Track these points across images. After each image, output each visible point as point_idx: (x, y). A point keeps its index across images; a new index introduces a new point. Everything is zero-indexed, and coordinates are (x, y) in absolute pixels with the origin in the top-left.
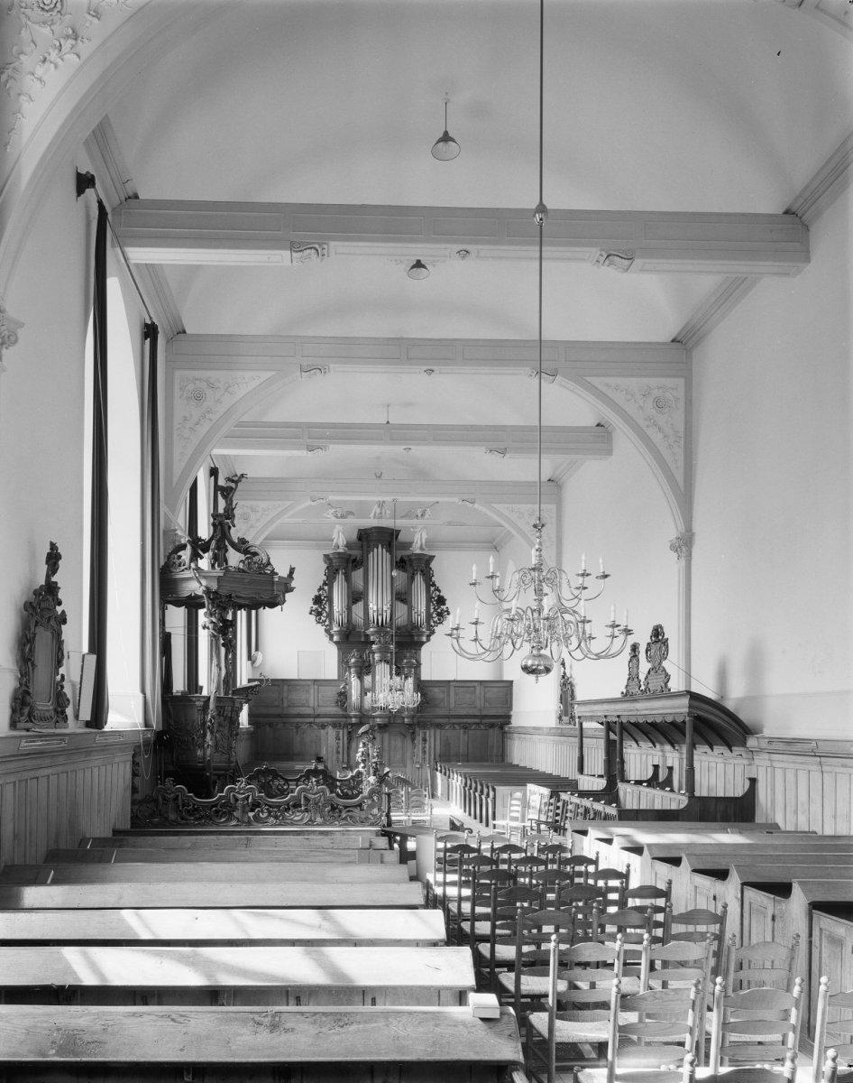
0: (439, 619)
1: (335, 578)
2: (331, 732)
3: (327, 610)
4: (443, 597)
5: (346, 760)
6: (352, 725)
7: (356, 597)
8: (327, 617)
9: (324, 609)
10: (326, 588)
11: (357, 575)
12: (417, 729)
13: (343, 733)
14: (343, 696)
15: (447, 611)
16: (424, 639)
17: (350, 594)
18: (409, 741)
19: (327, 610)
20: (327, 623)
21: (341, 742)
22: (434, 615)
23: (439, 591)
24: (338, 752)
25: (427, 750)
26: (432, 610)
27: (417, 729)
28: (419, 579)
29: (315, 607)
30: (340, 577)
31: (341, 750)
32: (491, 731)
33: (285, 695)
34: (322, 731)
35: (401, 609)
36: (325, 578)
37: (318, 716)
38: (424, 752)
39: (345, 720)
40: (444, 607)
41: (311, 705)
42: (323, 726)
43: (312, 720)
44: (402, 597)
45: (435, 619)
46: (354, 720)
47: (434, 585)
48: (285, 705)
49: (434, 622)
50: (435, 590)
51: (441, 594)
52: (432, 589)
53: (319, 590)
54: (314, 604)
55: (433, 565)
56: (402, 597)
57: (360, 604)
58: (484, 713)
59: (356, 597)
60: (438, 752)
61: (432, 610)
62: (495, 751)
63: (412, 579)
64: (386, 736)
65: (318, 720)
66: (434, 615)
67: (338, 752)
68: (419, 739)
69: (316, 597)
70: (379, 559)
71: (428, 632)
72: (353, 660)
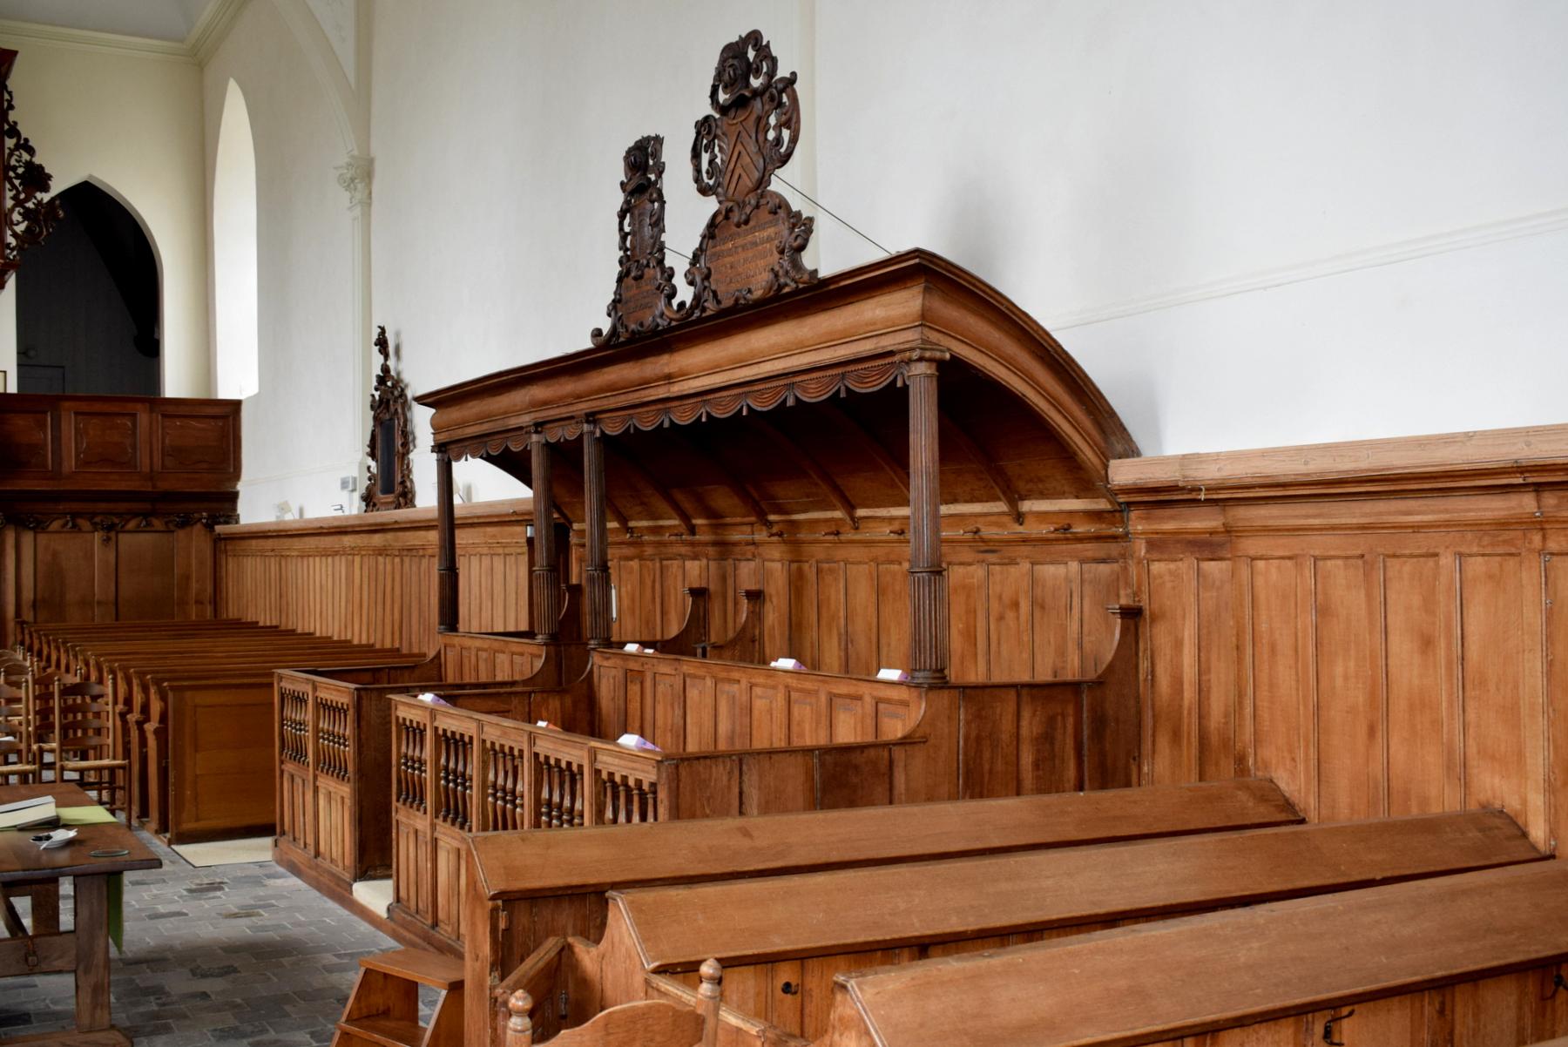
4: (41, 168)
22: (16, 217)
23: (31, 151)
26: (9, 203)
32: (181, 534)
47: (14, 132)
50: (18, 147)
51: (37, 160)
58: (164, 486)
60: (28, 594)
61: (9, 203)
62: (194, 586)
66: (16, 217)
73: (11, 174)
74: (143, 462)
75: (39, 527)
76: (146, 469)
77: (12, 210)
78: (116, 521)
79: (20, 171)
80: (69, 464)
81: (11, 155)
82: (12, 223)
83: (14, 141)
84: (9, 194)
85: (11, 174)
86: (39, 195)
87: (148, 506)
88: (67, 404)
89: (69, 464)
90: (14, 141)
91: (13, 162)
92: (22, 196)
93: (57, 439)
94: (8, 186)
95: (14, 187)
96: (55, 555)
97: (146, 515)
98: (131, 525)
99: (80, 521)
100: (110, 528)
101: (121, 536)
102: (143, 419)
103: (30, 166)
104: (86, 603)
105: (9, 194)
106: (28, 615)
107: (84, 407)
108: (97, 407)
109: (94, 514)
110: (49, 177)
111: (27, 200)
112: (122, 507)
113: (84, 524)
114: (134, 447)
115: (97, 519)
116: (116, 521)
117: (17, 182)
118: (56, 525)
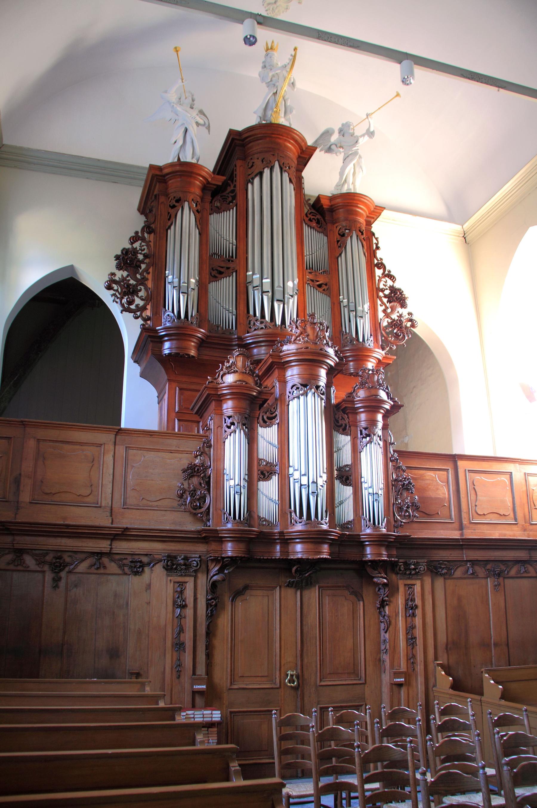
1: (171, 218)
5: (201, 670)
7: (218, 265)
8: (147, 300)
9: (142, 282)
11: (223, 224)
13: (197, 589)
14: (201, 477)
15: (411, 320)
19: (150, 284)
20: (148, 313)
21: (189, 612)
24: (179, 646)
25: (418, 633)
26: (381, 315)
29: (120, 274)
30: (186, 218)
31: (188, 637)
33: (27, 466)
37: (124, 534)
38: (411, 641)
39: (201, 548)
40: (404, 312)
41: (106, 502)
42: (137, 566)
43: (103, 545)
46: (230, 549)
47: (381, 265)
48: (25, 497)
50: (385, 275)
51: (397, 285)
52: (379, 272)
53: (134, 239)
54: (119, 267)
55: (375, 228)
60: (442, 638)
63: (337, 247)
64: (313, 595)
65: (122, 547)
67: (179, 646)
69: (125, 252)
72: (230, 379)
73: (381, 294)
78: (503, 568)
79: (387, 292)
81: (380, 281)
83: (381, 271)
85: (381, 294)
90: (381, 271)
91: (381, 286)
94: (379, 302)
98: (513, 572)
101: (506, 580)
103: (392, 288)
104: (485, 645)
105: (380, 309)
115: (488, 567)
116: (503, 568)
118: (458, 573)
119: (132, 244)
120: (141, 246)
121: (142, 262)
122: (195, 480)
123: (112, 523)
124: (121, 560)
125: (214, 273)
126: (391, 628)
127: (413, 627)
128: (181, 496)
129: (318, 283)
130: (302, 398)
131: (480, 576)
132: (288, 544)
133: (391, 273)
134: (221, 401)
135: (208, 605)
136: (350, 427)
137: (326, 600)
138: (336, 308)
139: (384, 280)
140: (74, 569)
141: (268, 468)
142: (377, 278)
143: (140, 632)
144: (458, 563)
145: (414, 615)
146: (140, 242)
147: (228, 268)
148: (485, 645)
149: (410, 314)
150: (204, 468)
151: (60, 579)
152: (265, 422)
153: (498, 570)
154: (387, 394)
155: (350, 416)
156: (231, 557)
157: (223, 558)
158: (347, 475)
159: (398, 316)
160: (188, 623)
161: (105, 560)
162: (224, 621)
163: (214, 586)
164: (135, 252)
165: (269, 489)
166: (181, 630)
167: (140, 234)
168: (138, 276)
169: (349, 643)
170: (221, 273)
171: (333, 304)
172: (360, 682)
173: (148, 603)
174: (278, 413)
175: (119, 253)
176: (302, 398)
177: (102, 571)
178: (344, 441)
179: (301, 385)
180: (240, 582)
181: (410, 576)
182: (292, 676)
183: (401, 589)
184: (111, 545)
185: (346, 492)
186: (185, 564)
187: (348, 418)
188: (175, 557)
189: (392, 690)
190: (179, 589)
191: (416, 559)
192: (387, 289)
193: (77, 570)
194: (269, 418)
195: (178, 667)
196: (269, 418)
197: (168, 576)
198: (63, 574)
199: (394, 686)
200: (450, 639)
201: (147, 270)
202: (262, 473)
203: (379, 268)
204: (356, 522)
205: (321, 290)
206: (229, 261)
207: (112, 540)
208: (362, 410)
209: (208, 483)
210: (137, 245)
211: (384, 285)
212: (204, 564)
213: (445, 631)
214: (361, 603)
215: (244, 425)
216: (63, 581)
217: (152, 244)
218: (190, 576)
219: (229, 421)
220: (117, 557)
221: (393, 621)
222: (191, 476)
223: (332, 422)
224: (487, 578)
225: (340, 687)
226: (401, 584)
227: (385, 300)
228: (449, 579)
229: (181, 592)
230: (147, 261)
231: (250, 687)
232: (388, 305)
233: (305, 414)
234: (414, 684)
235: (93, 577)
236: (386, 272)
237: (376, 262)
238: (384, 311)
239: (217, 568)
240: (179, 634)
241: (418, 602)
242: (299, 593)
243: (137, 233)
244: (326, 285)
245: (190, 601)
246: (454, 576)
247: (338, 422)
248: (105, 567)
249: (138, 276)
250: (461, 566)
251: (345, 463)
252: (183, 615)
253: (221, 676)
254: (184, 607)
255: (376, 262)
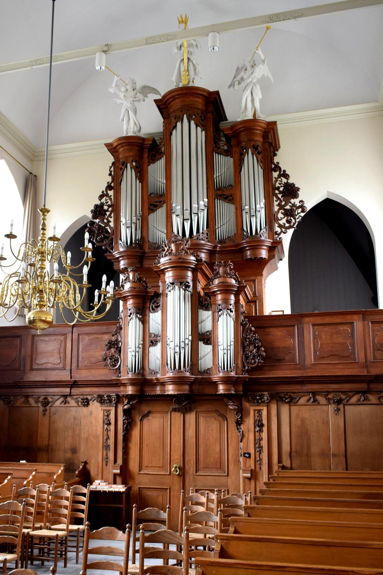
0: (288, 222)
2: (96, 410)
3: (112, 224)
5: (120, 461)
6: (130, 398)
7: (154, 201)
10: (111, 193)
12: (246, 405)
16: (264, 254)
17: (146, 198)
18: (233, 426)
19: (112, 224)
21: (112, 427)
22: (280, 215)
23: (286, 176)
26: (276, 208)
27: (246, 405)
28: (251, 164)
31: (111, 442)
34: (85, 409)
35: (225, 210)
36: (110, 179)
40: (296, 201)
44: (224, 193)
45: (281, 222)
46: (130, 390)
47: (277, 168)
49: (280, 226)
50: (280, 176)
51: (290, 181)
56: (224, 193)
57: (161, 212)
59: (154, 201)
60: (286, 448)
61: (276, 208)
64: (191, 417)
65: (75, 391)
66: (280, 215)
67: (106, 447)
68: (250, 422)
69: (96, 206)
70: (189, 138)
71: (268, 242)
74: (360, 356)
75: (292, 401)
76: (362, 360)
77: (278, 212)
78: (343, 397)
80: (310, 359)
81: (276, 181)
82: (278, 220)
83: (278, 173)
84: (276, 203)
85: (277, 192)
86: (292, 201)
87: (363, 386)
88: (307, 320)
89: (310, 359)
90: (278, 173)
91: (277, 185)
92: (283, 203)
93: (301, 343)
94: (275, 199)
95: (278, 198)
96: (303, 420)
97: (364, 393)
98: (354, 400)
99: (318, 397)
100: (339, 402)
101: (347, 407)
102: (358, 325)
104: (325, 454)
105: (276, 203)
106: (287, 462)
107: (318, 320)
108: (327, 320)
109: (329, 393)
110: (298, 189)
111: (286, 205)
112: (346, 387)
113: (321, 399)
114: (353, 345)
115: (330, 396)
116: (343, 397)
117: (280, 196)
118: (303, 401)
119: (100, 200)
120: (106, 200)
121: (107, 211)
122: (113, 350)
123: (71, 378)
124: (77, 398)
125: (151, 207)
126: (244, 440)
127: (261, 439)
128: (105, 360)
129: (225, 196)
130: (172, 291)
131: (321, 403)
132: (164, 385)
133: (287, 173)
134: (126, 300)
135: (124, 424)
136: (211, 305)
137: (202, 420)
138: (239, 211)
139: (280, 179)
140: (53, 404)
141: (155, 339)
142: (274, 179)
143: (87, 439)
144: (302, 394)
145: (261, 431)
146: (105, 197)
147: (160, 202)
148: (325, 454)
149: (301, 201)
150: (117, 342)
151: (46, 410)
152: (153, 309)
153: (337, 398)
154: (234, 279)
155: (211, 297)
156: (130, 395)
157: (127, 395)
158: (207, 338)
159: (290, 206)
160: (112, 434)
161: (69, 399)
162: (135, 433)
163: (126, 412)
164: (102, 205)
165: (155, 352)
166: (108, 438)
167: (105, 193)
168: (105, 221)
169: (218, 449)
170: (156, 206)
171: (236, 209)
172: (224, 475)
173: (91, 423)
174: (161, 303)
175: (93, 208)
176: (172, 291)
177: (67, 405)
178: (206, 316)
179: (171, 283)
180: (145, 409)
181: (258, 404)
182: (176, 468)
183: (252, 413)
184: (71, 390)
185: (205, 350)
186: (108, 400)
187: (210, 299)
188: (103, 396)
189: (244, 482)
190: (106, 414)
191: (260, 392)
192: (282, 186)
193: (54, 405)
194: (156, 307)
195: (106, 459)
196: (156, 307)
197: (101, 406)
198: (48, 408)
199: (246, 479)
200: (293, 449)
201: (110, 216)
202: (152, 342)
203: (275, 171)
204: (213, 368)
205: (227, 200)
206: (162, 196)
207: (71, 388)
208: (218, 292)
209: (120, 351)
210: (103, 200)
211: (279, 184)
212: (119, 399)
213: (289, 443)
214: (226, 422)
215: (138, 314)
216: (48, 411)
217: (112, 197)
218: (113, 406)
219: (129, 312)
220: (75, 397)
221: (246, 435)
222: (110, 348)
223: (197, 303)
224: (328, 405)
225: (210, 477)
226: (252, 410)
227: (280, 196)
228: (293, 405)
229: (108, 416)
230: (110, 209)
231: (151, 473)
232: (282, 199)
233: (175, 302)
234: (261, 479)
235: (63, 408)
236: (282, 172)
237: (273, 166)
238: (279, 205)
239: (127, 401)
240: (107, 439)
241: (265, 422)
242: (182, 416)
243: (103, 192)
244: (231, 196)
245: (113, 422)
246: (298, 404)
247: (202, 303)
248: (69, 403)
249: (105, 221)
250: (303, 396)
251: (207, 330)
252: (109, 429)
253: (133, 465)
254: (109, 424)
255: (273, 166)
